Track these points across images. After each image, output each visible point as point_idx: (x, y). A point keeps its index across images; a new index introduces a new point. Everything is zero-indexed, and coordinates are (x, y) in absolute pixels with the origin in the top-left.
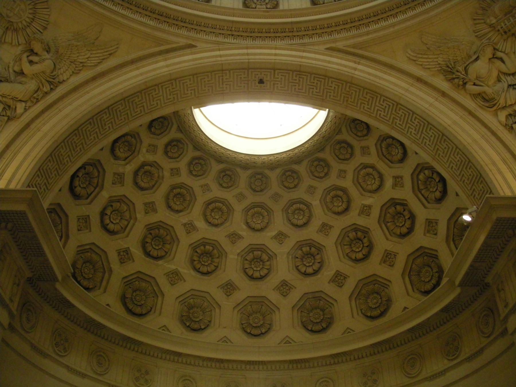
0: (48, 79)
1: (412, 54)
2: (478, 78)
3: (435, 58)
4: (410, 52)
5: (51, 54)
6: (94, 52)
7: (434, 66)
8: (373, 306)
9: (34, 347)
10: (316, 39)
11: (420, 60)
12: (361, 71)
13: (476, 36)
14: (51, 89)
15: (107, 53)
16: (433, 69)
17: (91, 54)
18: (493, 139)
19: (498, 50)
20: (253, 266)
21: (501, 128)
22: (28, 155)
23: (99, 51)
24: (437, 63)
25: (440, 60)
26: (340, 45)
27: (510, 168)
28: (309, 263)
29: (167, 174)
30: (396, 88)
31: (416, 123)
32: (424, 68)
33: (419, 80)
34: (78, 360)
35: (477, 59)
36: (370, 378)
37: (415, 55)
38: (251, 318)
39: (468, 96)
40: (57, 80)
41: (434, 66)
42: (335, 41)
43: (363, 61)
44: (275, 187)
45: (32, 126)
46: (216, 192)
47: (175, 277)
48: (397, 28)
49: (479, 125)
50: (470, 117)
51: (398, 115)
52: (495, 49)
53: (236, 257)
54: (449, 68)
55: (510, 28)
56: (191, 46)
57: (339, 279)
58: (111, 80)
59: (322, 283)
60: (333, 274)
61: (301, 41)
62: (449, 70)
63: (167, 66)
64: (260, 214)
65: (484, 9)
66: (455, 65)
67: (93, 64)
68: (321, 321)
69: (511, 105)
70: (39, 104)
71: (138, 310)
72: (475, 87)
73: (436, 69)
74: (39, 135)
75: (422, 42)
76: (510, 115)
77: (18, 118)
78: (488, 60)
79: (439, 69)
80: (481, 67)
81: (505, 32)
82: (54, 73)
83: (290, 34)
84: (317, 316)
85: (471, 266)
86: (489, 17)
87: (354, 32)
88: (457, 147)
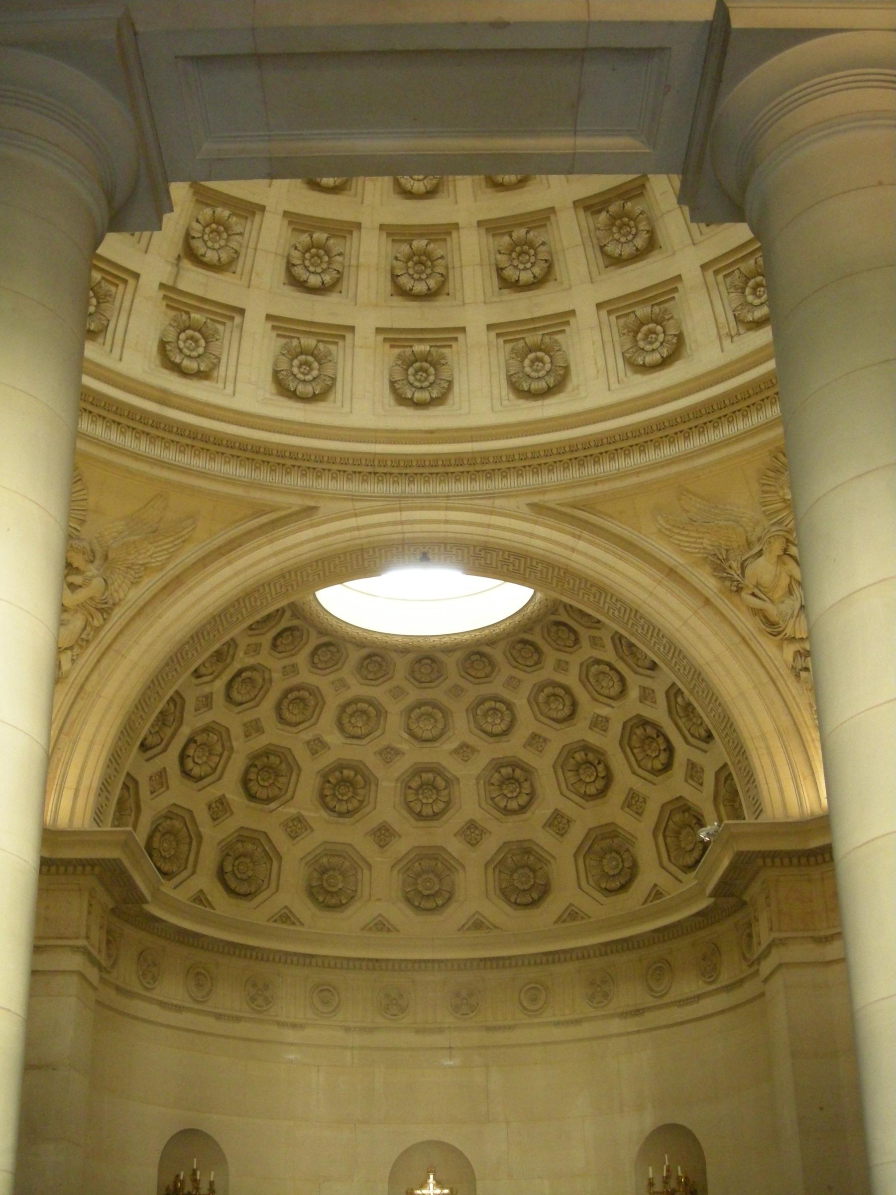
0: (99, 606)
1: (664, 524)
2: (757, 585)
3: (699, 538)
4: (661, 522)
5: (97, 562)
6: (160, 543)
8: (611, 873)
9: (118, 989)
10: (512, 483)
11: (676, 536)
13: (764, 512)
14: (104, 619)
15: (181, 540)
17: (156, 547)
20: (421, 797)
21: (785, 672)
22: (92, 743)
23: (167, 540)
25: (706, 542)
26: (551, 499)
28: (512, 792)
29: (276, 676)
33: (671, 573)
35: (760, 553)
36: (599, 989)
37: (667, 527)
38: (419, 881)
40: (111, 602)
42: (542, 491)
44: (453, 676)
45: (88, 688)
46: (357, 689)
47: (297, 827)
50: (743, 647)
52: (788, 541)
53: (394, 784)
56: (310, 510)
57: (558, 823)
58: (190, 590)
59: (532, 827)
60: (549, 815)
62: (719, 562)
63: (275, 554)
64: (430, 715)
66: (727, 555)
67: (160, 563)
69: (802, 639)
70: (90, 650)
71: (243, 888)
72: (753, 599)
73: (700, 555)
75: (682, 507)
77: (66, 678)
78: (775, 559)
80: (763, 569)
82: (107, 594)
83: (471, 469)
84: (523, 880)
86: (782, 487)
87: (574, 473)
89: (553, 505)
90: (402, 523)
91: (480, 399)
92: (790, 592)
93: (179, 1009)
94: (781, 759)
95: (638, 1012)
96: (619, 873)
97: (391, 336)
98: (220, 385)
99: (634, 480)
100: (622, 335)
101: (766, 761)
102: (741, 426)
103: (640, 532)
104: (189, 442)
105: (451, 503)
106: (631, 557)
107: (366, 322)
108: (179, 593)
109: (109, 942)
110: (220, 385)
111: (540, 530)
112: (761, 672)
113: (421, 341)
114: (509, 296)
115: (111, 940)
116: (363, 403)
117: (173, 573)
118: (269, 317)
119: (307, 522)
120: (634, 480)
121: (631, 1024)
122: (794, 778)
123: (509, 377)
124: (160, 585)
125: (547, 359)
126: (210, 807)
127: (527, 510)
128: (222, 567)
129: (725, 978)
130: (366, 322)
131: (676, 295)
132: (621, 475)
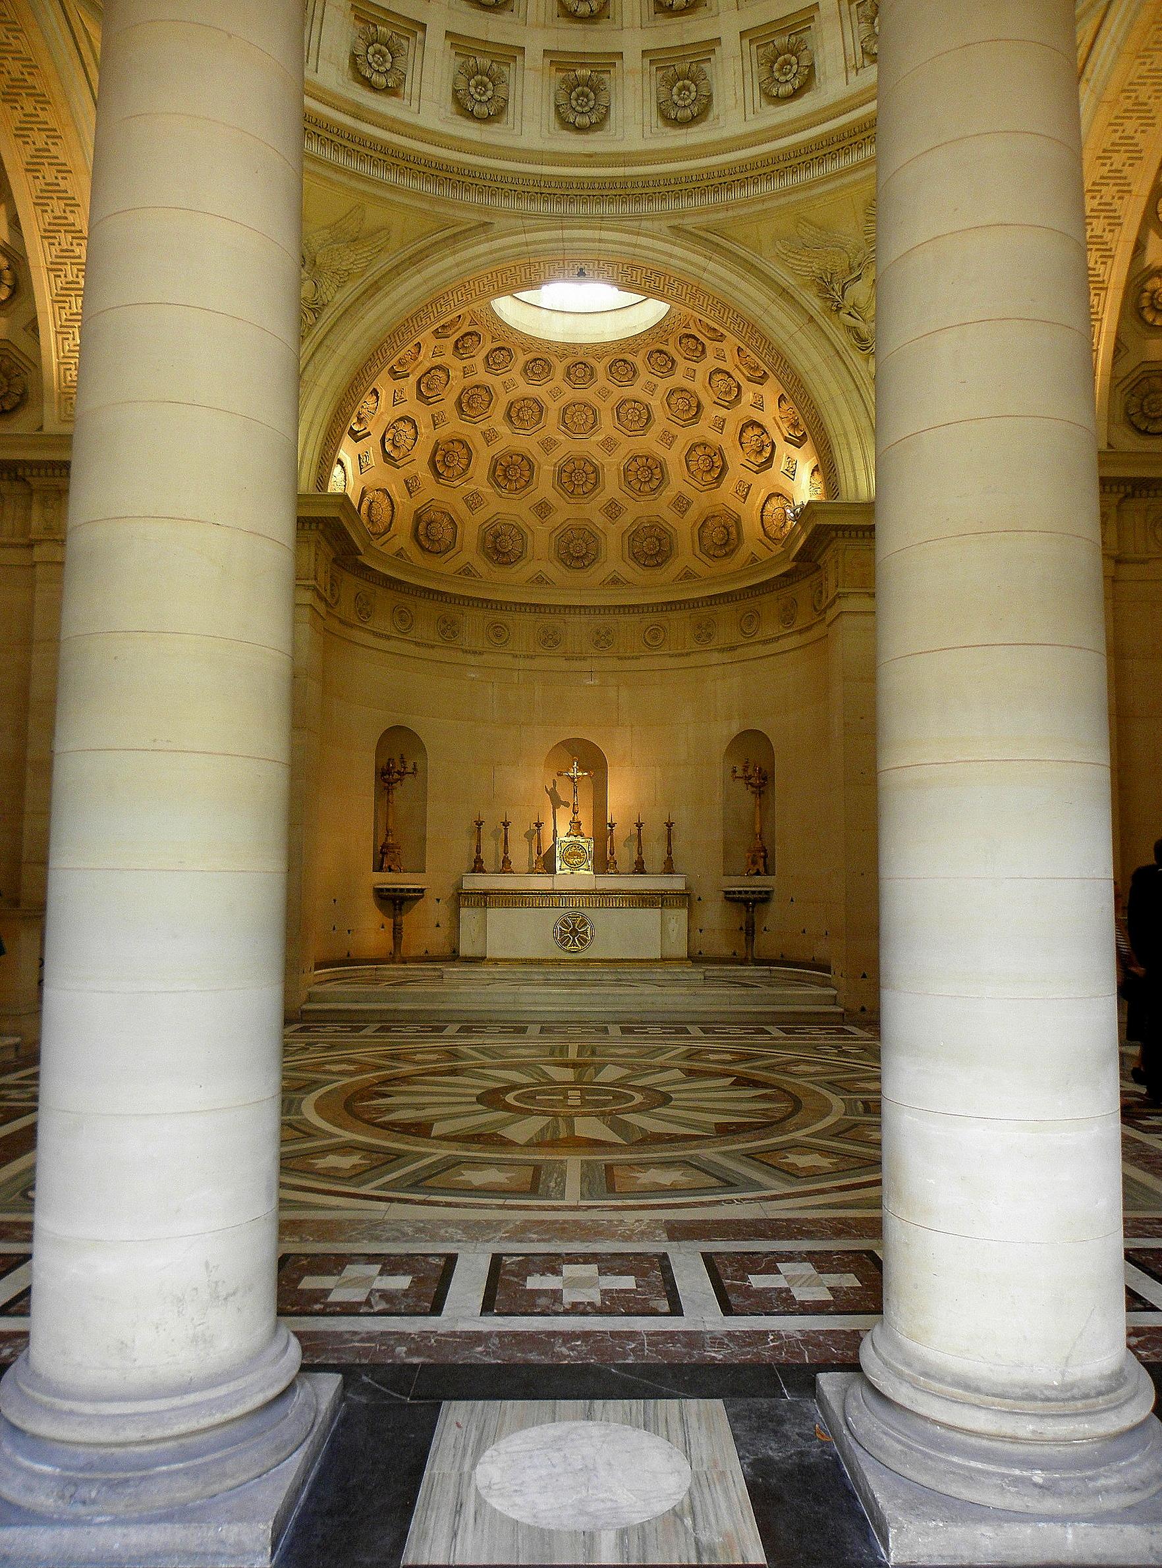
9: (341, 621)
10: (656, 206)
12: (711, 273)
18: (855, 395)
21: (868, 381)
26: (689, 222)
33: (784, 293)
34: (382, 624)
35: (858, 278)
46: (524, 389)
58: (387, 294)
63: (457, 265)
68: (656, 555)
71: (436, 547)
74: (316, 393)
80: (860, 292)
87: (711, 199)
89: (690, 228)
90: (563, 240)
91: (633, 125)
93: (388, 638)
94: (857, 454)
95: (732, 649)
96: (725, 544)
97: (558, 60)
98: (406, 102)
99: (759, 207)
100: (760, 65)
104: (381, 156)
105: (605, 224)
106: (752, 279)
107: (536, 42)
108: (377, 297)
109: (332, 585)
110: (406, 102)
111: (678, 251)
112: (848, 380)
113: (583, 65)
114: (662, 21)
115: (334, 582)
116: (531, 124)
117: (371, 280)
118: (448, 34)
119: (483, 237)
120: (759, 207)
121: (726, 657)
123: (659, 104)
124: (362, 288)
125: (693, 87)
126: (406, 482)
127: (668, 231)
128: (412, 275)
129: (800, 623)
130: (536, 42)
131: (812, 25)
132: (750, 202)
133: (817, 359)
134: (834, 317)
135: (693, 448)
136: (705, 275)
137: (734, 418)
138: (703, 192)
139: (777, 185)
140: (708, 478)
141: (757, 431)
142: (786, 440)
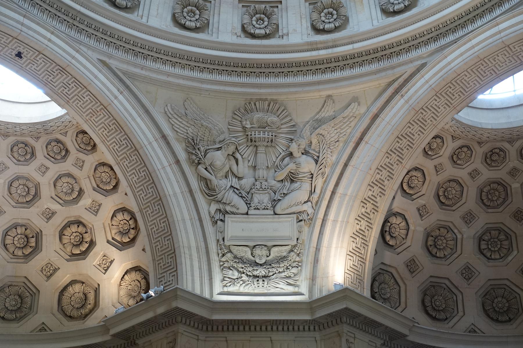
4: (169, 108)
7: (182, 133)
16: (180, 134)
19: (238, 151)
24: (186, 131)
26: (113, 63)
27: (200, 259)
30: (142, 137)
31: (143, 174)
32: (173, 129)
33: (164, 137)
35: (219, 149)
37: (172, 113)
39: (196, 175)
41: (182, 133)
42: (110, 56)
43: (126, 93)
48: (170, 79)
49: (193, 206)
50: (189, 195)
51: (130, 157)
54: (194, 142)
55: (257, 140)
61: (77, 36)
62: (193, 144)
65: (246, 110)
76: (220, 210)
79: (185, 137)
80: (218, 158)
81: (251, 140)
83: (71, 21)
85: (133, 327)
86: (246, 120)
87: (130, 57)
88: (166, 217)
90: (22, 24)
92: (226, 177)
101: (188, 262)
102: (235, 79)
103: (154, 108)
122: (201, 277)
133: (178, 191)
134: (193, 169)
135: (15, 226)
136: (115, 102)
137: (64, 214)
138: (127, 51)
139: (178, 71)
140: (20, 253)
141: (81, 229)
142: (108, 242)
